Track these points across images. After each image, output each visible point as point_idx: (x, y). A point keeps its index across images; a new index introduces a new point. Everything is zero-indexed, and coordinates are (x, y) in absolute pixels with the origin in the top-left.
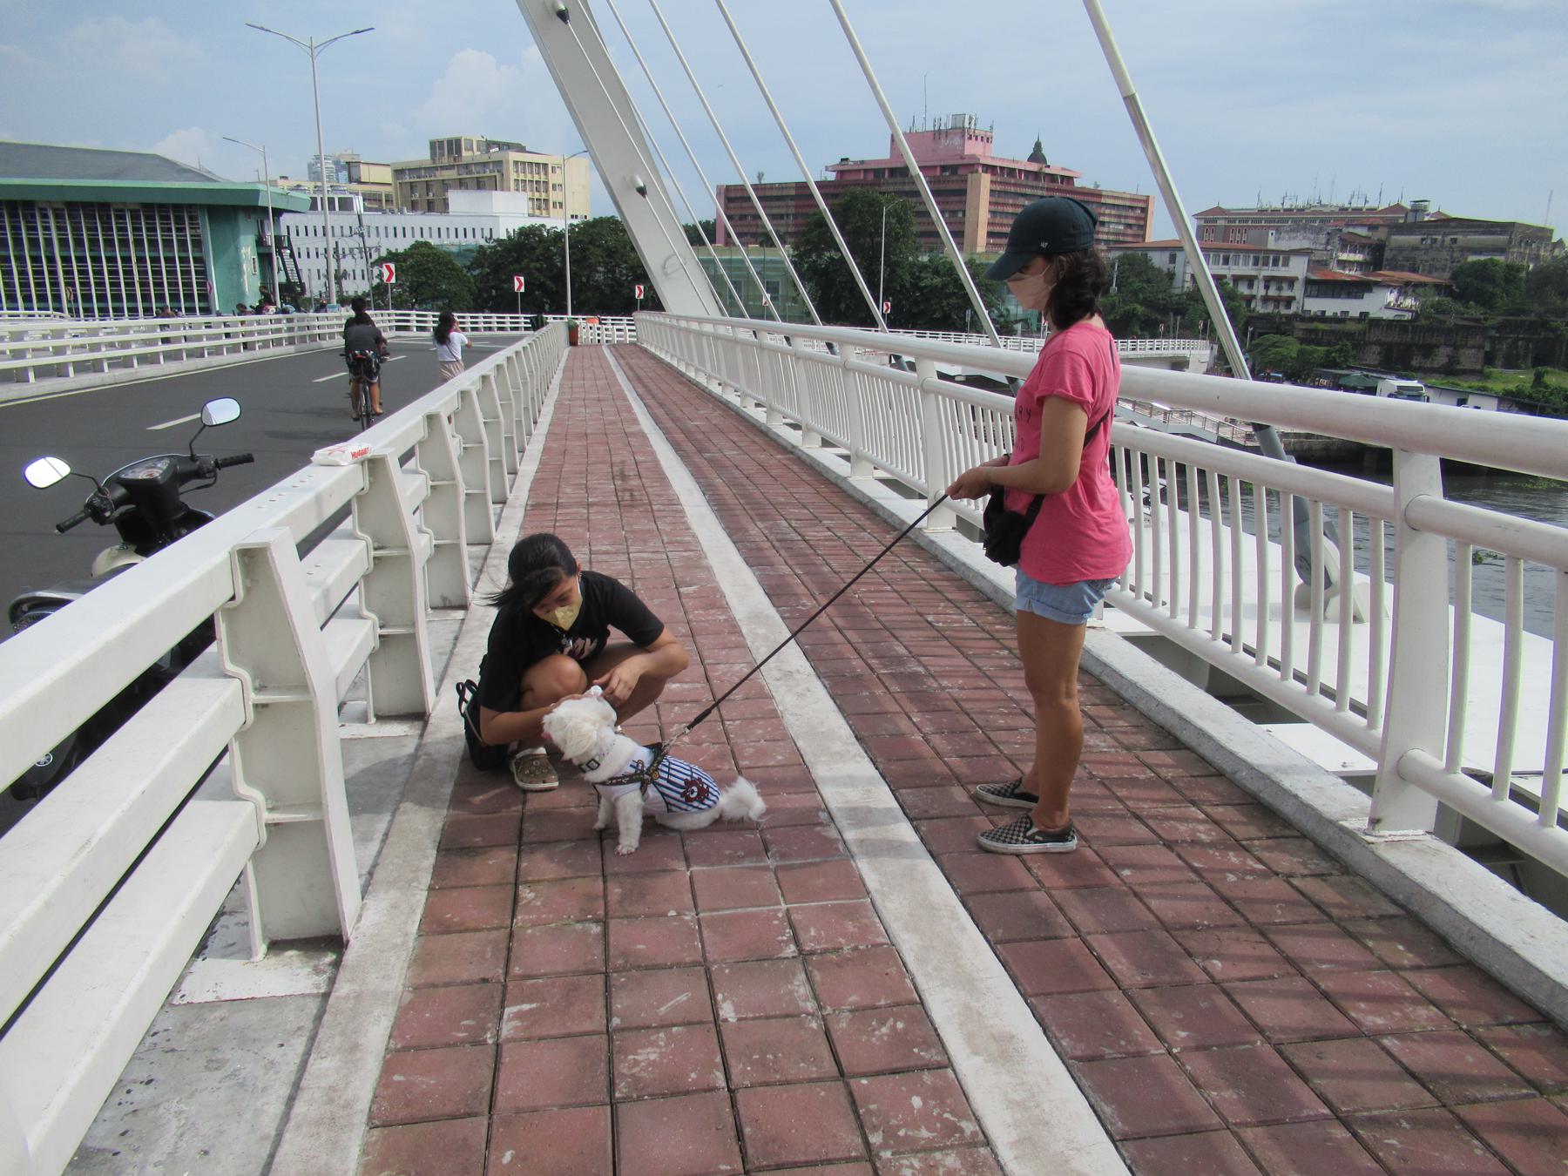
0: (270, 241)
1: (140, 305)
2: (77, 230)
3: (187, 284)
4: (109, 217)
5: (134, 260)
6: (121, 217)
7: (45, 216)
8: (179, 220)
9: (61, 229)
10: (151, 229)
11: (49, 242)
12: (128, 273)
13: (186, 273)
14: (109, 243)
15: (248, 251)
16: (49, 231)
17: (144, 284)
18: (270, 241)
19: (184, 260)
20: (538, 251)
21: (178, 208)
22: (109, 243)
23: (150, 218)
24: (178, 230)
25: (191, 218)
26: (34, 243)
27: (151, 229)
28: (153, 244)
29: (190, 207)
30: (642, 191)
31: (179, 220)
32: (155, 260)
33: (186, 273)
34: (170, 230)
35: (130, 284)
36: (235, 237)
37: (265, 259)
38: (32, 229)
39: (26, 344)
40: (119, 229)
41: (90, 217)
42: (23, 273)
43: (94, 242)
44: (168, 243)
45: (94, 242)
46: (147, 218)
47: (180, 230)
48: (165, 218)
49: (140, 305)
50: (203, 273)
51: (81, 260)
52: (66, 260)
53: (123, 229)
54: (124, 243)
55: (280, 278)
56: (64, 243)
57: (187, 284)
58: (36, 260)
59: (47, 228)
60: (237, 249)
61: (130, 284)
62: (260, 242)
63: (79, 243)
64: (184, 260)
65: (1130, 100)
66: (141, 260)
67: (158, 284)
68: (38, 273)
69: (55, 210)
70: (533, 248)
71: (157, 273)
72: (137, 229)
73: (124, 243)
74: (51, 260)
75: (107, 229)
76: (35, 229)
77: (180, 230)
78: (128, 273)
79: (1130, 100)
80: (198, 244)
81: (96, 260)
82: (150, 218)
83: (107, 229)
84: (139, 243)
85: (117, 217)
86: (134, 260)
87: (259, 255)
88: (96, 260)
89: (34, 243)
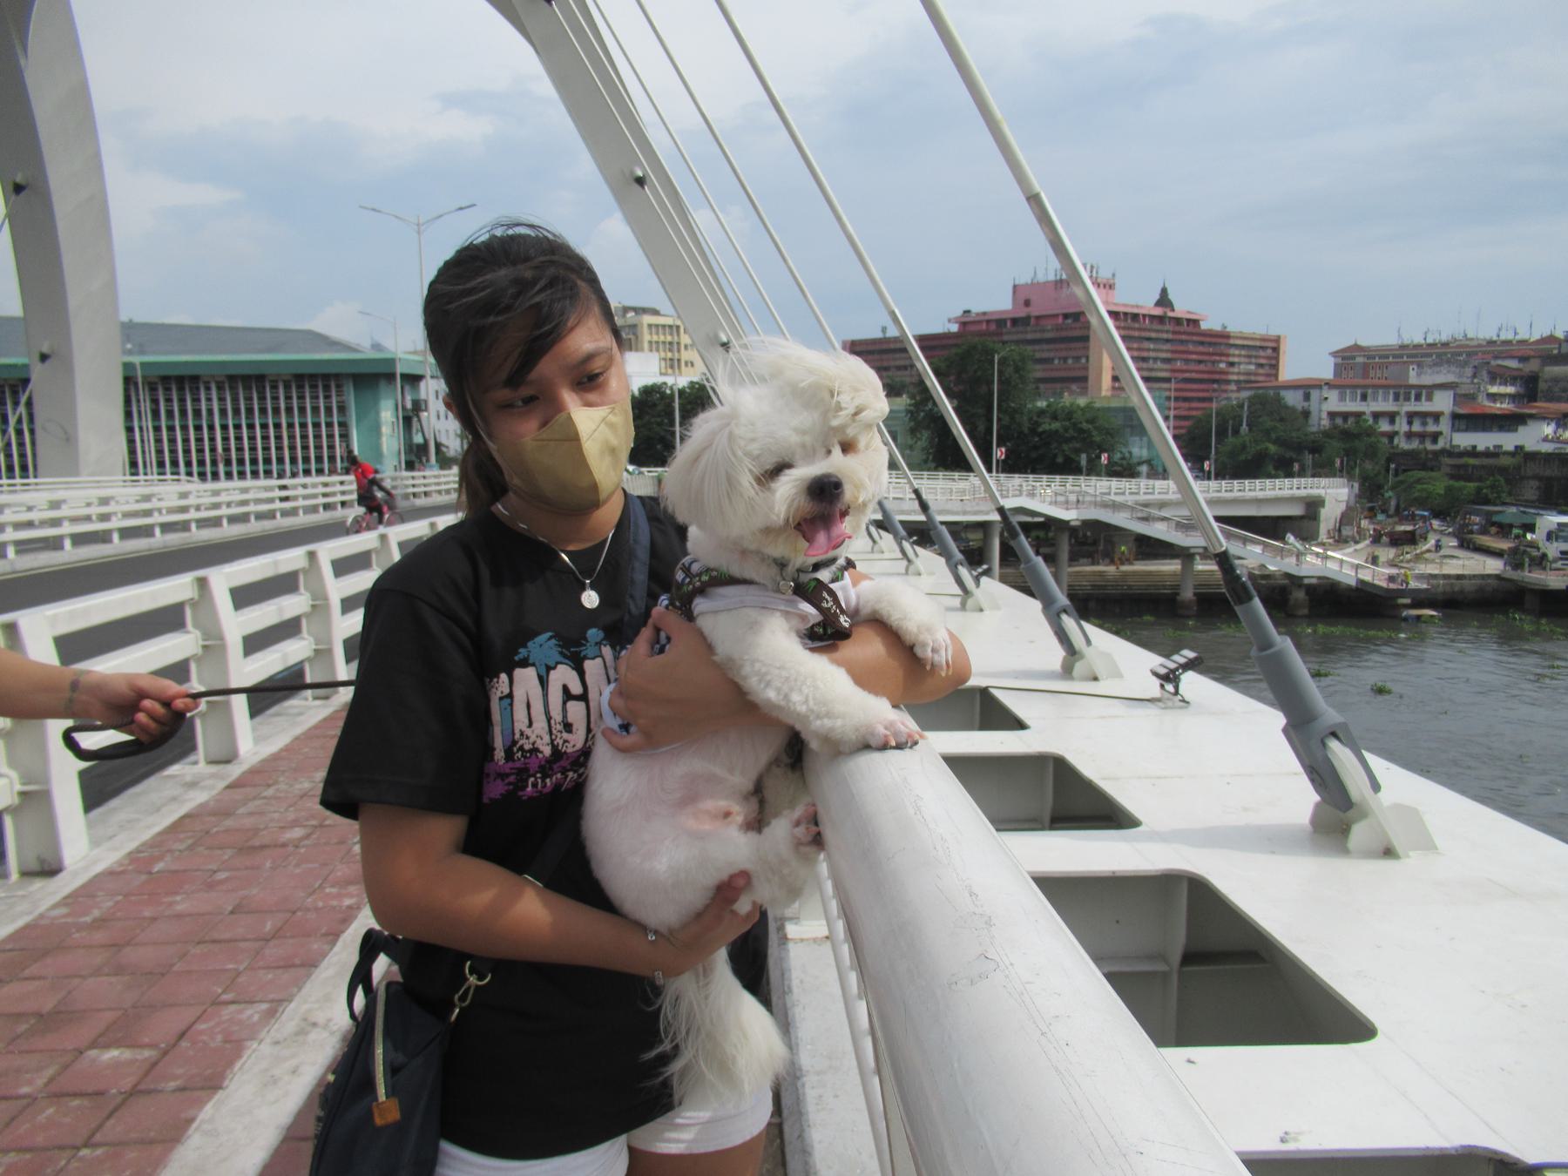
2: (235, 400)
5: (284, 425)
6: (274, 387)
7: (208, 389)
8: (327, 388)
9: (222, 399)
10: (301, 397)
11: (210, 412)
12: (279, 438)
14: (263, 411)
15: (387, 415)
16: (211, 402)
17: (292, 448)
18: (409, 405)
19: (329, 425)
20: (660, 408)
21: (326, 377)
22: (263, 411)
23: (300, 387)
26: (197, 413)
27: (301, 397)
28: (302, 410)
29: (337, 376)
30: (726, 346)
31: (327, 388)
32: (303, 426)
35: (279, 448)
38: (196, 400)
39: (65, 511)
41: (248, 388)
42: (186, 441)
43: (250, 411)
44: (315, 410)
45: (250, 411)
47: (327, 397)
48: (314, 387)
51: (238, 427)
52: (224, 428)
53: (275, 398)
54: (276, 411)
56: (223, 412)
58: (198, 428)
59: (209, 400)
60: (378, 413)
61: (279, 448)
63: (237, 412)
64: (329, 425)
65: (1034, 200)
67: (305, 448)
68: (199, 440)
70: (655, 405)
71: (304, 437)
72: (288, 398)
73: (276, 411)
74: (211, 428)
75: (262, 398)
76: (199, 400)
77: (327, 397)
78: (279, 438)
79: (1034, 200)
80: (342, 409)
81: (251, 427)
82: (300, 387)
83: (262, 398)
84: (289, 410)
86: (284, 425)
88: (251, 427)
89: (197, 413)
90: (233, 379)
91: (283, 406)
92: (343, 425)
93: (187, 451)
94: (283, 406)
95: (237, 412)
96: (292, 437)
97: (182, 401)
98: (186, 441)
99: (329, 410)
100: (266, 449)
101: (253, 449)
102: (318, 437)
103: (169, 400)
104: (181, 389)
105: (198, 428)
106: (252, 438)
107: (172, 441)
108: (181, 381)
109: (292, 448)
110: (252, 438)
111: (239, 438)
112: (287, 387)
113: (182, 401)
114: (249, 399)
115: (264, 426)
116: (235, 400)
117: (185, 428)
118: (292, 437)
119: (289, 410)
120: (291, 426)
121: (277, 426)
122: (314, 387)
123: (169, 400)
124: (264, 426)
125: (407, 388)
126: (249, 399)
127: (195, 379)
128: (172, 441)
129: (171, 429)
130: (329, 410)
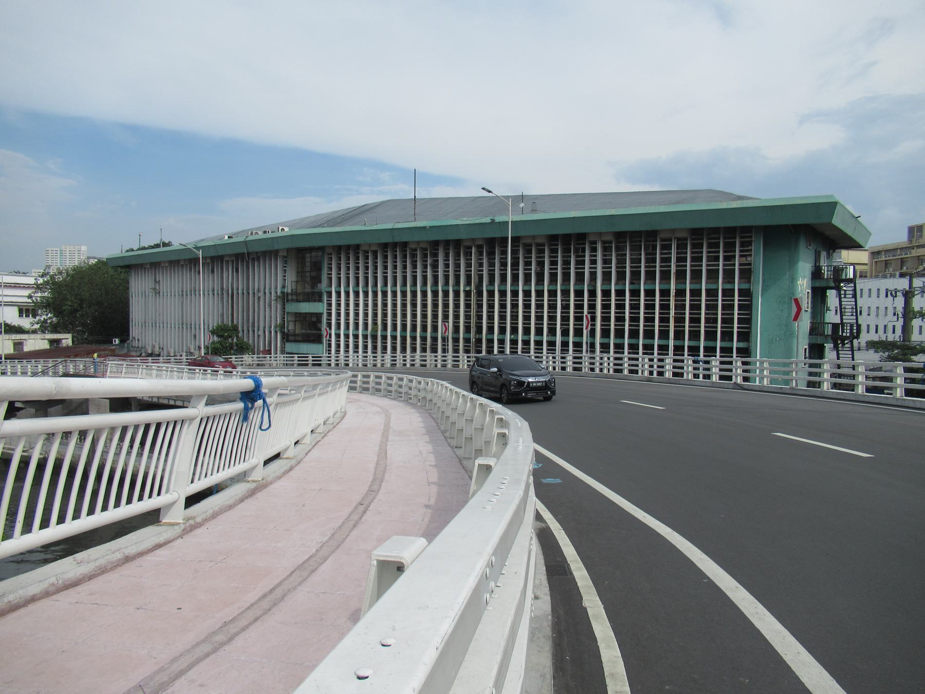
0: (826, 272)
1: (671, 343)
2: (621, 262)
3: (727, 321)
4: (655, 248)
6: (666, 247)
7: (594, 250)
8: (730, 247)
9: (607, 262)
11: (593, 275)
12: (665, 307)
13: (728, 307)
14: (650, 276)
16: (595, 264)
17: (680, 320)
19: (728, 293)
21: (730, 231)
22: (650, 276)
23: (697, 246)
24: (726, 258)
25: (742, 245)
26: (580, 277)
27: (697, 259)
28: (697, 275)
31: (730, 247)
32: (696, 293)
33: (728, 307)
34: (717, 259)
35: (664, 320)
36: (793, 263)
37: (819, 295)
40: (663, 260)
41: (636, 249)
42: (566, 307)
43: (636, 275)
45: (636, 275)
46: (694, 246)
48: (714, 246)
49: (671, 343)
50: (747, 308)
51: (620, 293)
52: (606, 293)
53: (666, 260)
55: (832, 317)
56: (607, 276)
57: (727, 321)
58: (579, 293)
59: (594, 262)
60: (793, 280)
61: (664, 320)
62: (816, 274)
63: (621, 276)
66: (680, 293)
67: (695, 320)
69: (604, 242)
71: (695, 307)
72: (681, 260)
74: (593, 293)
75: (651, 260)
76: (583, 263)
78: (665, 307)
80: (747, 274)
81: (635, 293)
82: (697, 246)
83: (651, 260)
84: (681, 275)
85: (664, 247)
87: (814, 289)
88: (635, 293)
89: (580, 277)
90: (620, 237)
91: (673, 269)
92: (746, 294)
93: (565, 319)
94: (673, 269)
95: (621, 276)
96: (680, 307)
97: (567, 263)
98: (566, 307)
99: (729, 275)
100: (649, 320)
101: (635, 319)
102: (711, 307)
103: (554, 263)
104: (567, 251)
105: (579, 293)
106: (635, 307)
107: (553, 307)
108: (566, 239)
109: (680, 320)
110: (635, 307)
111: (620, 306)
112: (681, 246)
113: (567, 263)
114: (636, 261)
115: (650, 293)
116: (621, 262)
117: (566, 293)
118: (680, 307)
119: (681, 275)
120: (680, 293)
121: (665, 293)
122: (714, 246)
123: (554, 263)
124: (650, 293)
125: (823, 254)
126: (636, 261)
127: (581, 237)
128: (553, 307)
129: (553, 293)
130: (729, 275)
